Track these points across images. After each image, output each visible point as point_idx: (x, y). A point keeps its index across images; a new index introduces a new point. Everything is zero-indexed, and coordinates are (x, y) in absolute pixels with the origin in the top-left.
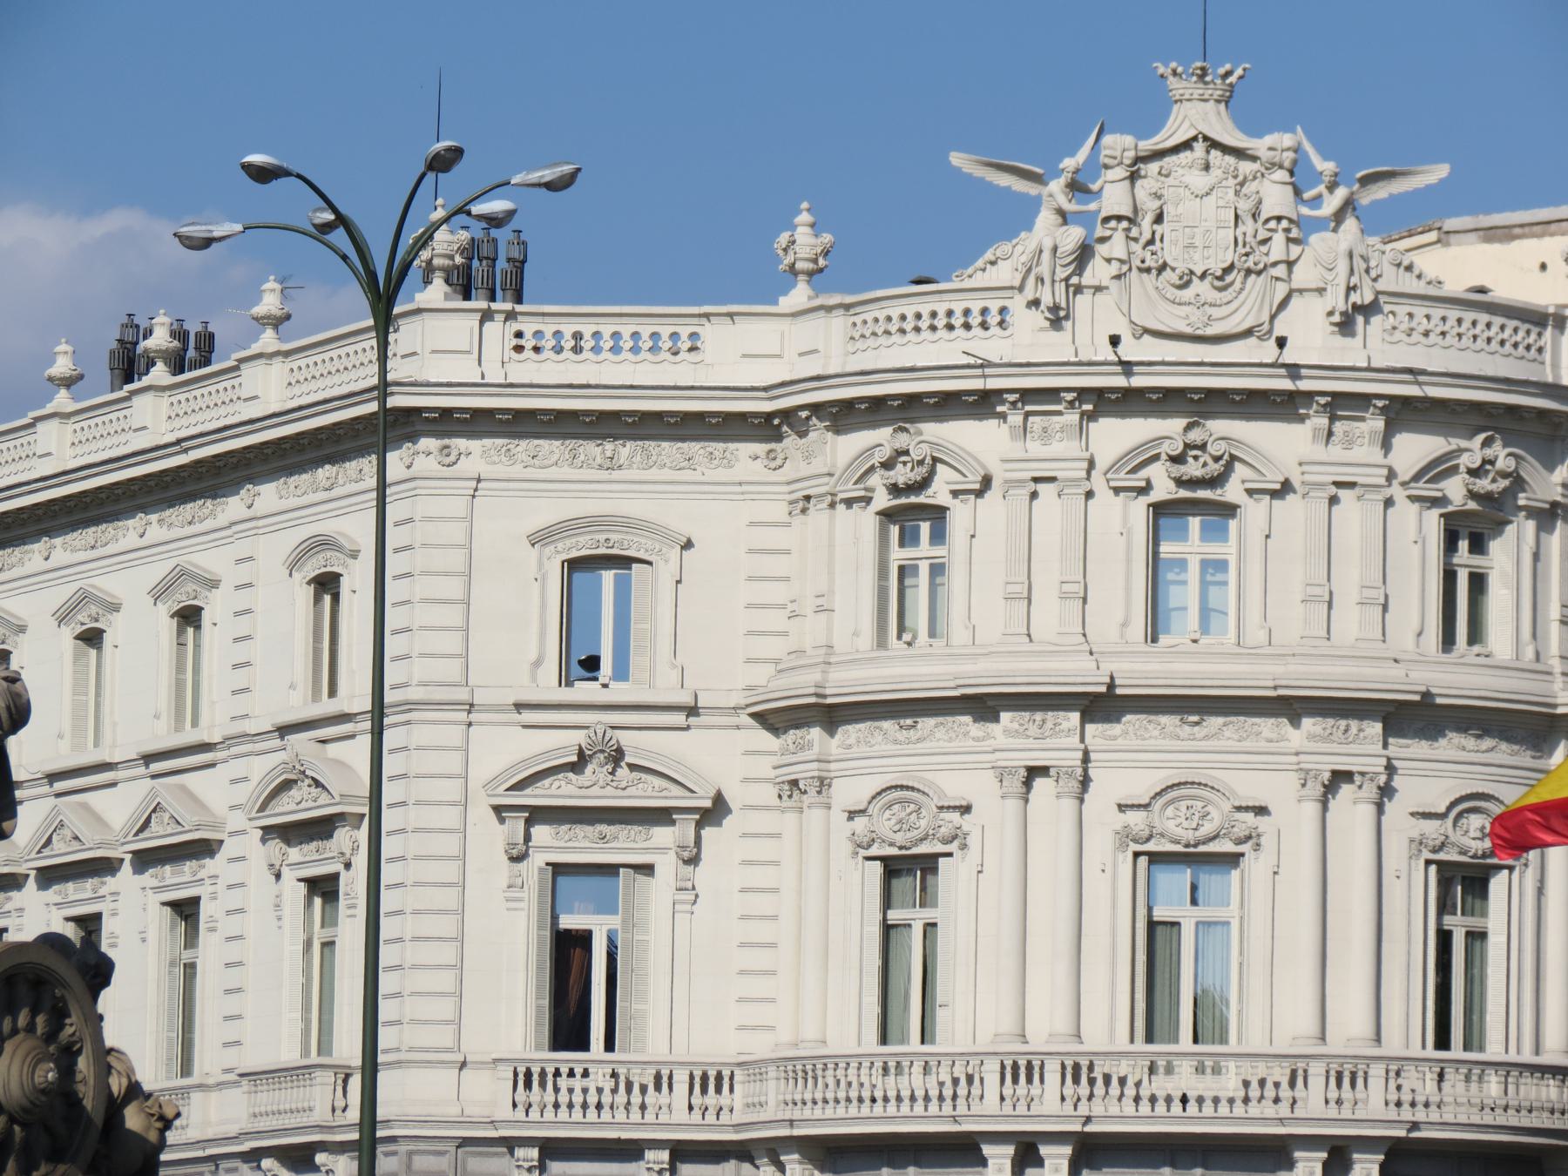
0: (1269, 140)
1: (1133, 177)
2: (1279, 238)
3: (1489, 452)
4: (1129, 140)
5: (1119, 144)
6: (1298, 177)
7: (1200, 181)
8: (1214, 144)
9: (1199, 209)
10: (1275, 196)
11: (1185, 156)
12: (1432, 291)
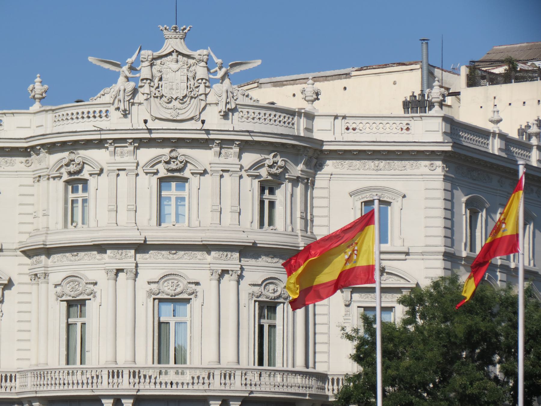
1: (152, 65)
3: (275, 159)
4: (150, 52)
5: (147, 53)
11: (169, 58)
12: (255, 104)
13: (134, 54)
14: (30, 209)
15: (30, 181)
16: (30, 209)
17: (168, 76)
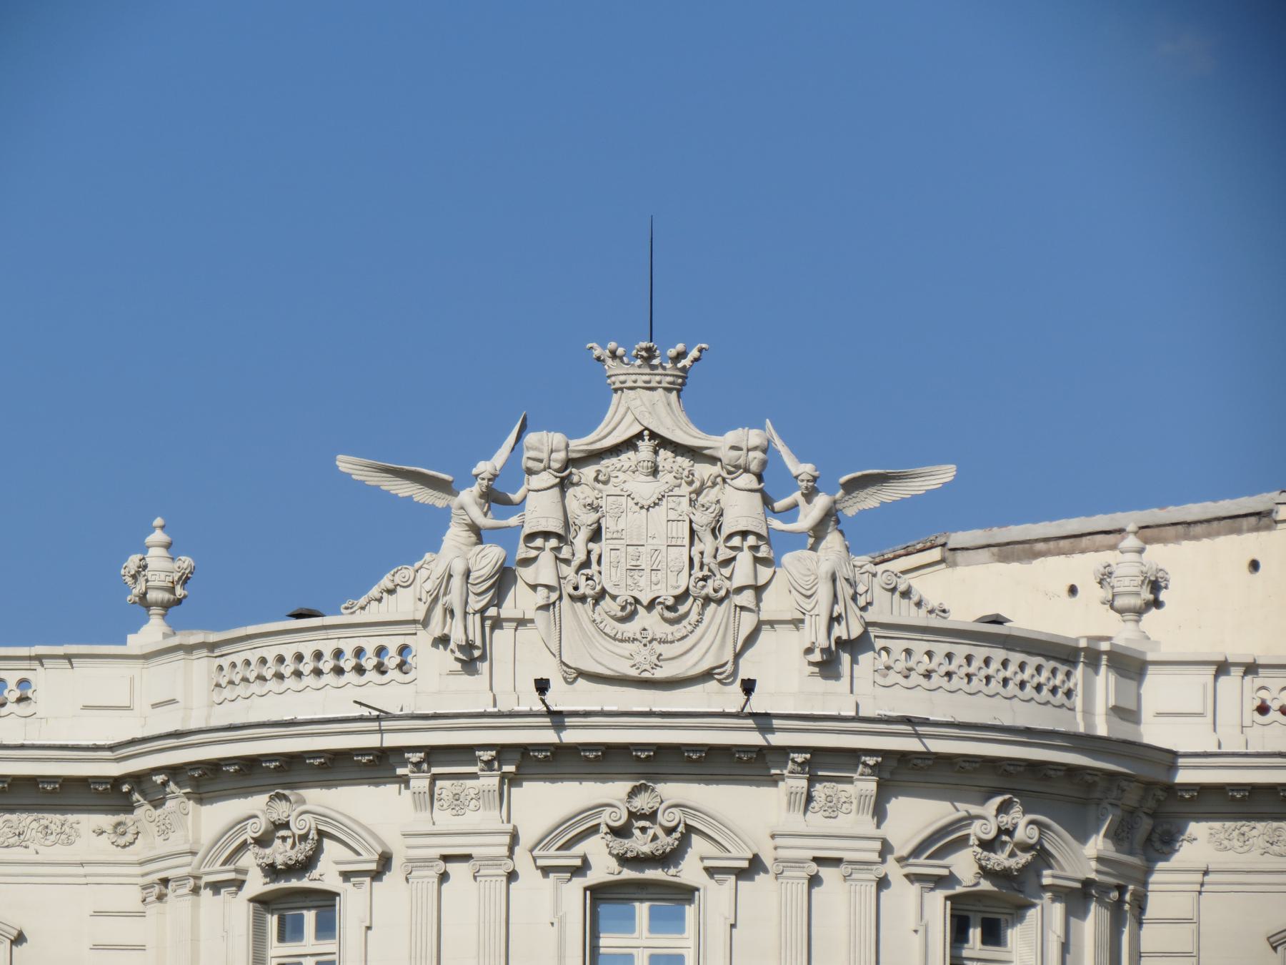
0: (732, 437)
1: (564, 484)
2: (744, 559)
3: (1005, 820)
4: (558, 438)
7: (646, 488)
8: (663, 443)
10: (741, 507)
11: (627, 458)
12: (935, 622)
13: (499, 445)
15: (130, 897)
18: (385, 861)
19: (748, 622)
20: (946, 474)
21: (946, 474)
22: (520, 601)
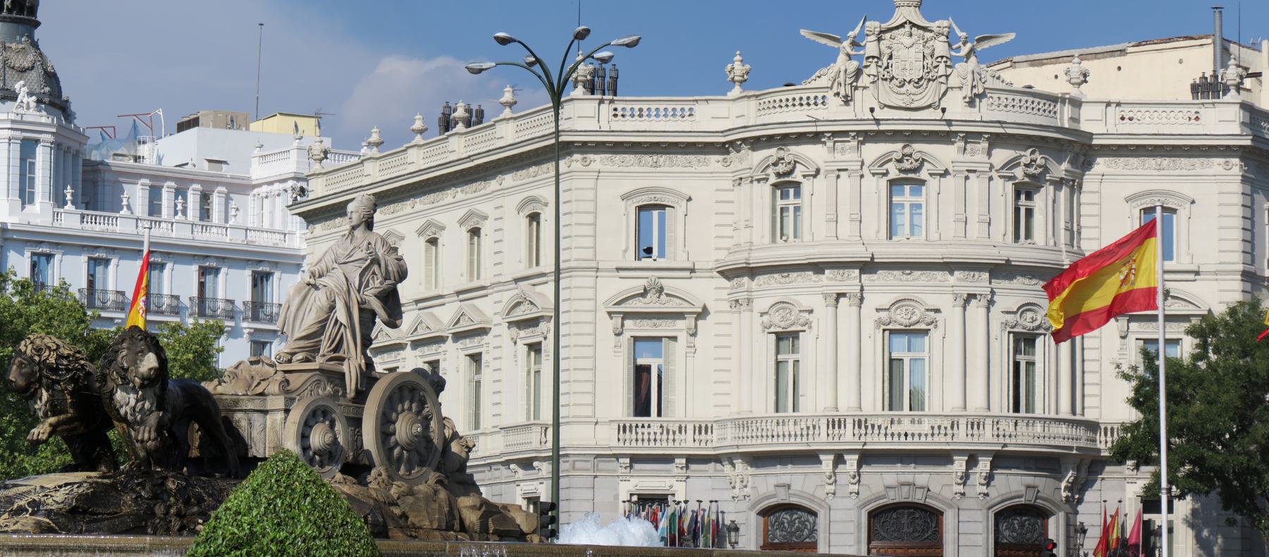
0: (937, 23)
1: (879, 40)
2: (942, 66)
3: (1033, 157)
4: (877, 24)
5: (873, 25)
6: (950, 39)
7: (907, 41)
8: (914, 25)
9: (908, 54)
10: (941, 48)
11: (901, 31)
12: (1008, 88)
14: (728, 220)
15: (729, 184)
16: (728, 220)
17: (900, 53)
18: (818, 171)
19: (943, 88)
20: (1012, 36)
21: (1012, 36)
22: (864, 80)
